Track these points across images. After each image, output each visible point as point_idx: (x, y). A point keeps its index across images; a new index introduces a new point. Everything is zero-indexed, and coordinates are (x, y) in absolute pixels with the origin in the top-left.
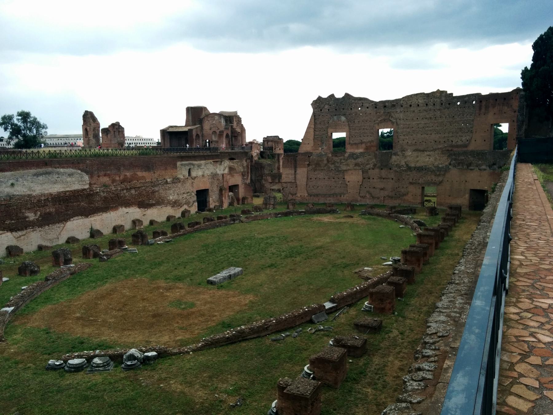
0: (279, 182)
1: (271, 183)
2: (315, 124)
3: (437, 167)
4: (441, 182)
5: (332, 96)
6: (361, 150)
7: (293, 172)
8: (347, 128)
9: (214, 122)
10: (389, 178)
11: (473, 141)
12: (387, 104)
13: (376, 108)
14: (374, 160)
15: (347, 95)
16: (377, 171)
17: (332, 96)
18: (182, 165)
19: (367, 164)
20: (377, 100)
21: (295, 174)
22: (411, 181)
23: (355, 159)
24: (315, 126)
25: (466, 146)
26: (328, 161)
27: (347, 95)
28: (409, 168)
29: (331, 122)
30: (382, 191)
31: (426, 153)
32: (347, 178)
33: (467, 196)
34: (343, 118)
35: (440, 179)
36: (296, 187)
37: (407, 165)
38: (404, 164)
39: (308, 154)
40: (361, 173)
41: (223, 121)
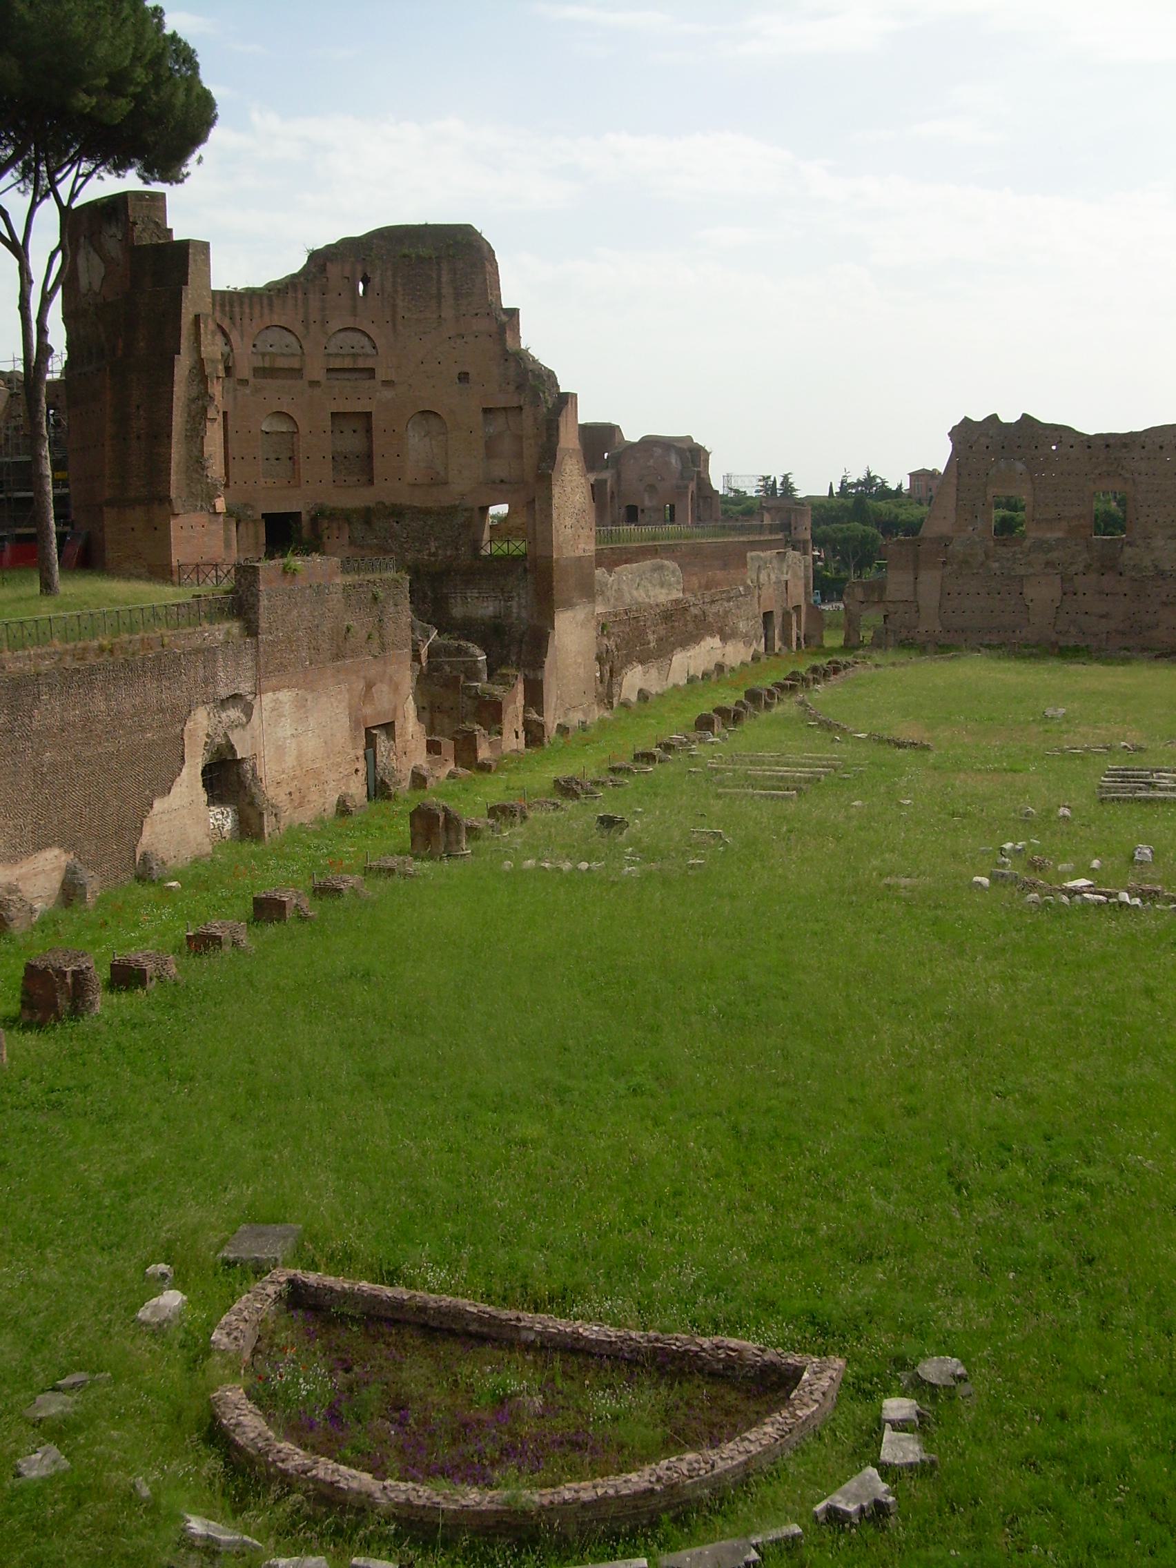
0: (880, 601)
1: (862, 602)
5: (994, 418)
6: (1059, 534)
7: (912, 579)
9: (651, 462)
10: (1117, 594)
12: (1111, 441)
13: (1089, 447)
14: (1086, 556)
15: (1025, 417)
17: (994, 418)
18: (752, 559)
19: (1071, 564)
20: (1090, 431)
21: (915, 583)
22: (1164, 599)
24: (958, 479)
26: (987, 556)
27: (1025, 417)
30: (1104, 620)
32: (1029, 592)
34: (1020, 466)
36: (918, 611)
38: (1149, 564)
39: (944, 542)
40: (1057, 579)
41: (674, 460)
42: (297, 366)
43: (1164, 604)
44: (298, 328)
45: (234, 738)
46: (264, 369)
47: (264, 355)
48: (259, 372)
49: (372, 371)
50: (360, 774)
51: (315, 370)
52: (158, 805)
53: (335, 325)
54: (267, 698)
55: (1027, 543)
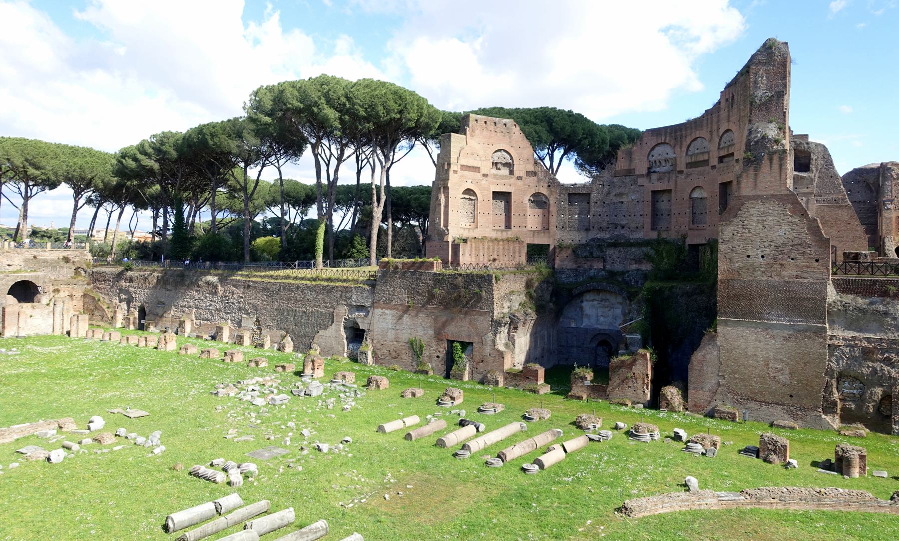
42: (706, 158)
44: (707, 136)
45: (359, 321)
46: (691, 163)
47: (691, 156)
48: (690, 165)
49: (732, 154)
50: (440, 359)
51: (714, 161)
52: (321, 332)
53: (721, 131)
54: (378, 311)
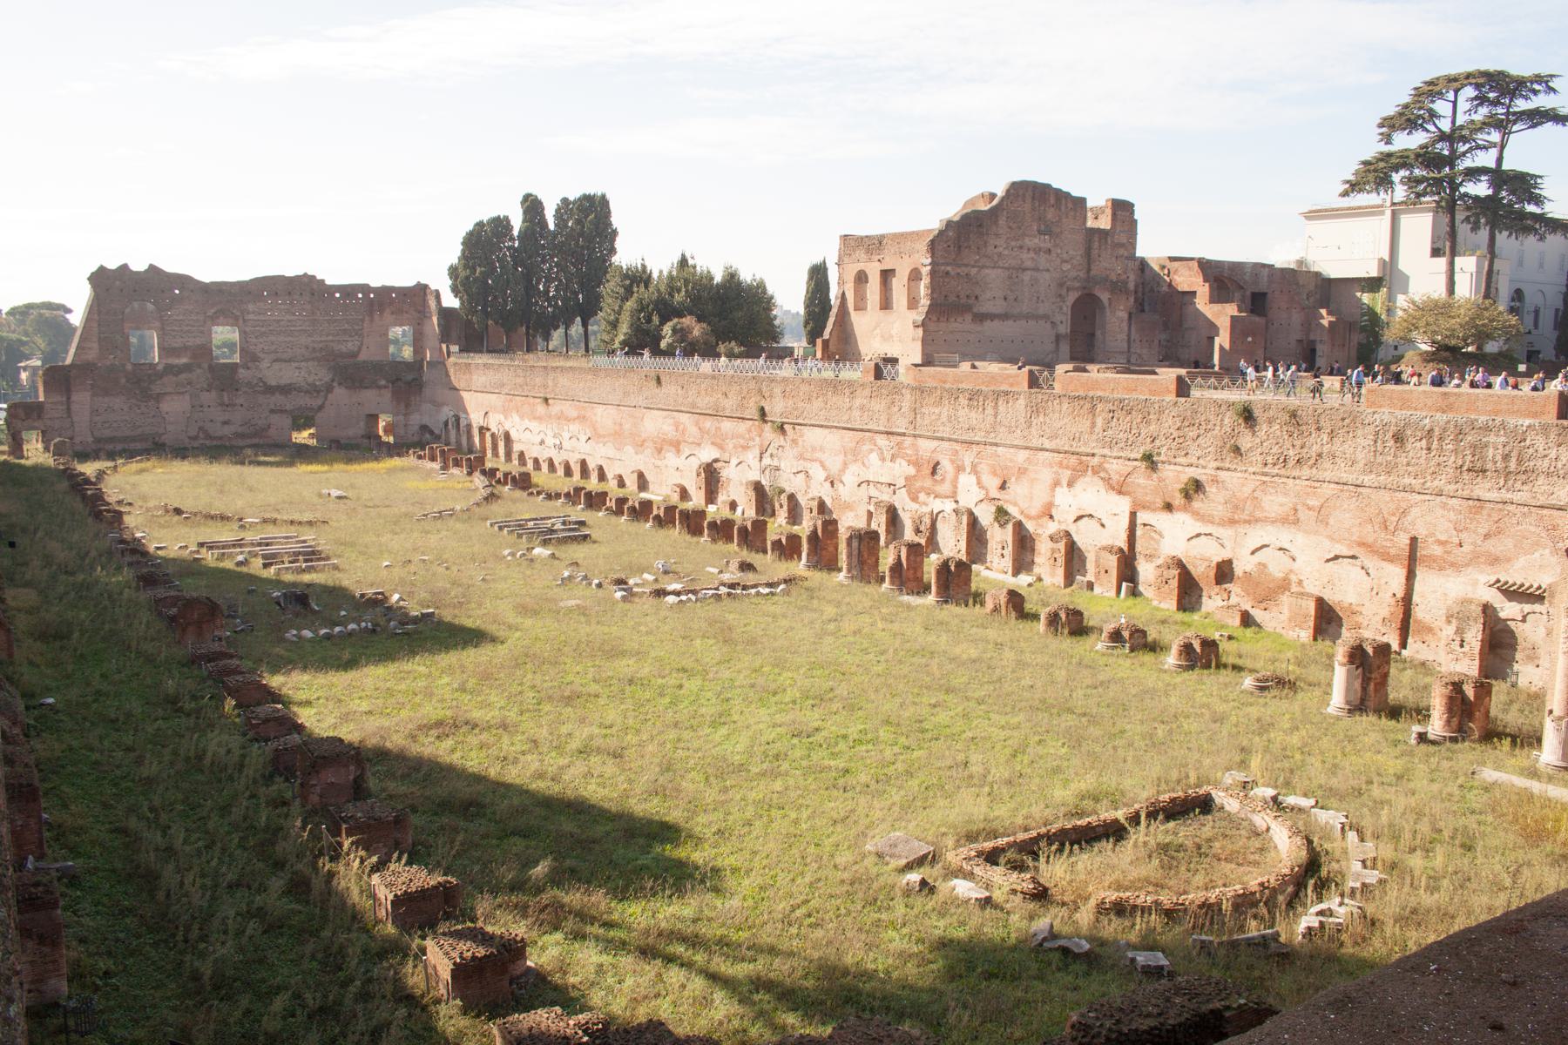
2: (99, 312)
3: (313, 385)
4: (321, 408)
5: (125, 267)
6: (184, 360)
8: (158, 324)
11: (364, 348)
15: (152, 268)
16: (214, 394)
17: (125, 267)
22: (273, 407)
23: (176, 375)
25: (354, 355)
28: (270, 390)
29: (127, 310)
31: (296, 364)
33: (362, 424)
34: (150, 307)
35: (319, 402)
37: (265, 383)
40: (187, 397)
43: (272, 411)
55: (160, 367)
